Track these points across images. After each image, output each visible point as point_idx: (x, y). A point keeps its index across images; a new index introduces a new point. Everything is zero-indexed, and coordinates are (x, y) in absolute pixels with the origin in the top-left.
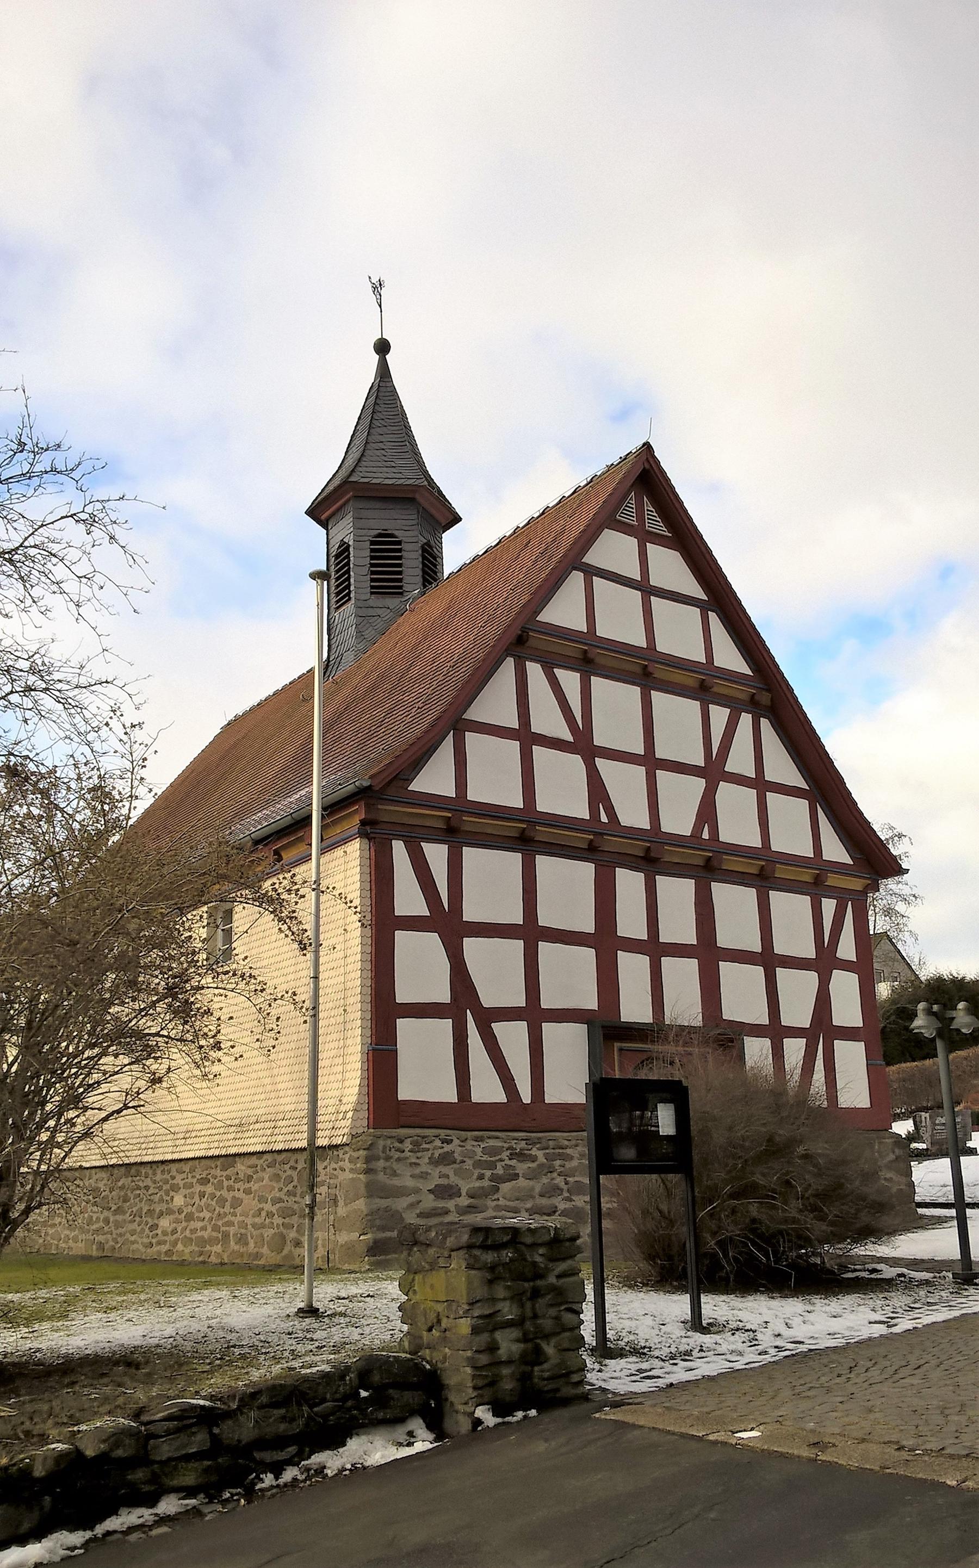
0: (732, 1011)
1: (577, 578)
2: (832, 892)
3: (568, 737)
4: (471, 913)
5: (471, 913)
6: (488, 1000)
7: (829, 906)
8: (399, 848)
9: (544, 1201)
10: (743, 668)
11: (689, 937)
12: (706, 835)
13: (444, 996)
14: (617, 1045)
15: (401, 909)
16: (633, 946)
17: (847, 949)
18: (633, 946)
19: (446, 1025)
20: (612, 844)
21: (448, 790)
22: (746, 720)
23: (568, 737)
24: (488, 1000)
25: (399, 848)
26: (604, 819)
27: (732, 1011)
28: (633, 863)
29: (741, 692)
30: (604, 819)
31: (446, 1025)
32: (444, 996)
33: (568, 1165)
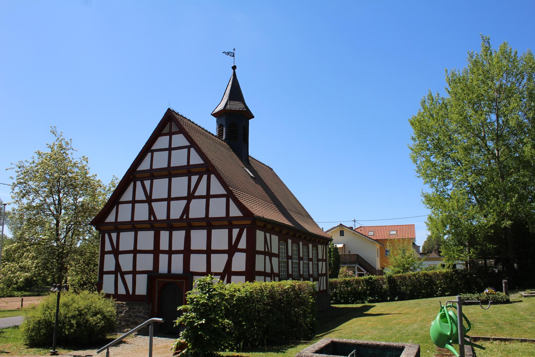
0: (193, 269)
1: (149, 154)
2: (236, 227)
3: (145, 199)
4: (121, 249)
5: (121, 249)
6: (123, 269)
7: (235, 232)
8: (106, 235)
9: (128, 319)
10: (201, 162)
11: (181, 247)
12: (185, 217)
13: (113, 269)
14: (157, 280)
15: (106, 250)
16: (164, 252)
17: (242, 244)
18: (164, 252)
19: (113, 276)
20: (156, 225)
21: (113, 220)
22: (205, 177)
23: (145, 199)
24: (123, 269)
25: (106, 235)
26: (152, 219)
27: (193, 269)
28: (165, 229)
29: (204, 169)
30: (152, 219)
31: (113, 276)
32: (113, 269)
33: (135, 310)
